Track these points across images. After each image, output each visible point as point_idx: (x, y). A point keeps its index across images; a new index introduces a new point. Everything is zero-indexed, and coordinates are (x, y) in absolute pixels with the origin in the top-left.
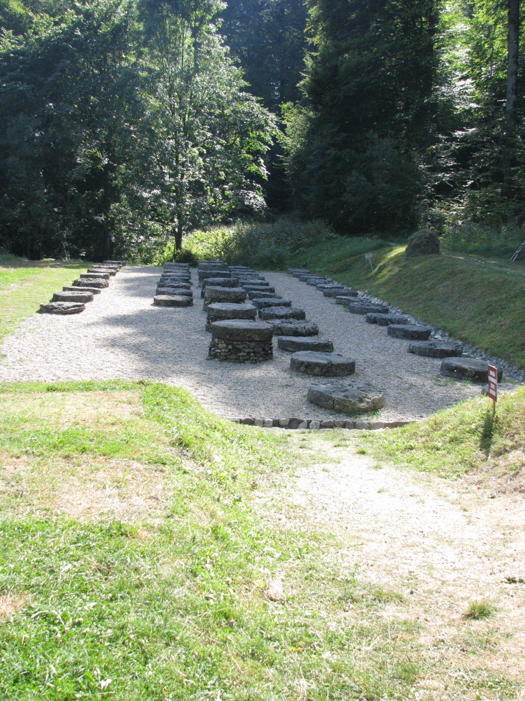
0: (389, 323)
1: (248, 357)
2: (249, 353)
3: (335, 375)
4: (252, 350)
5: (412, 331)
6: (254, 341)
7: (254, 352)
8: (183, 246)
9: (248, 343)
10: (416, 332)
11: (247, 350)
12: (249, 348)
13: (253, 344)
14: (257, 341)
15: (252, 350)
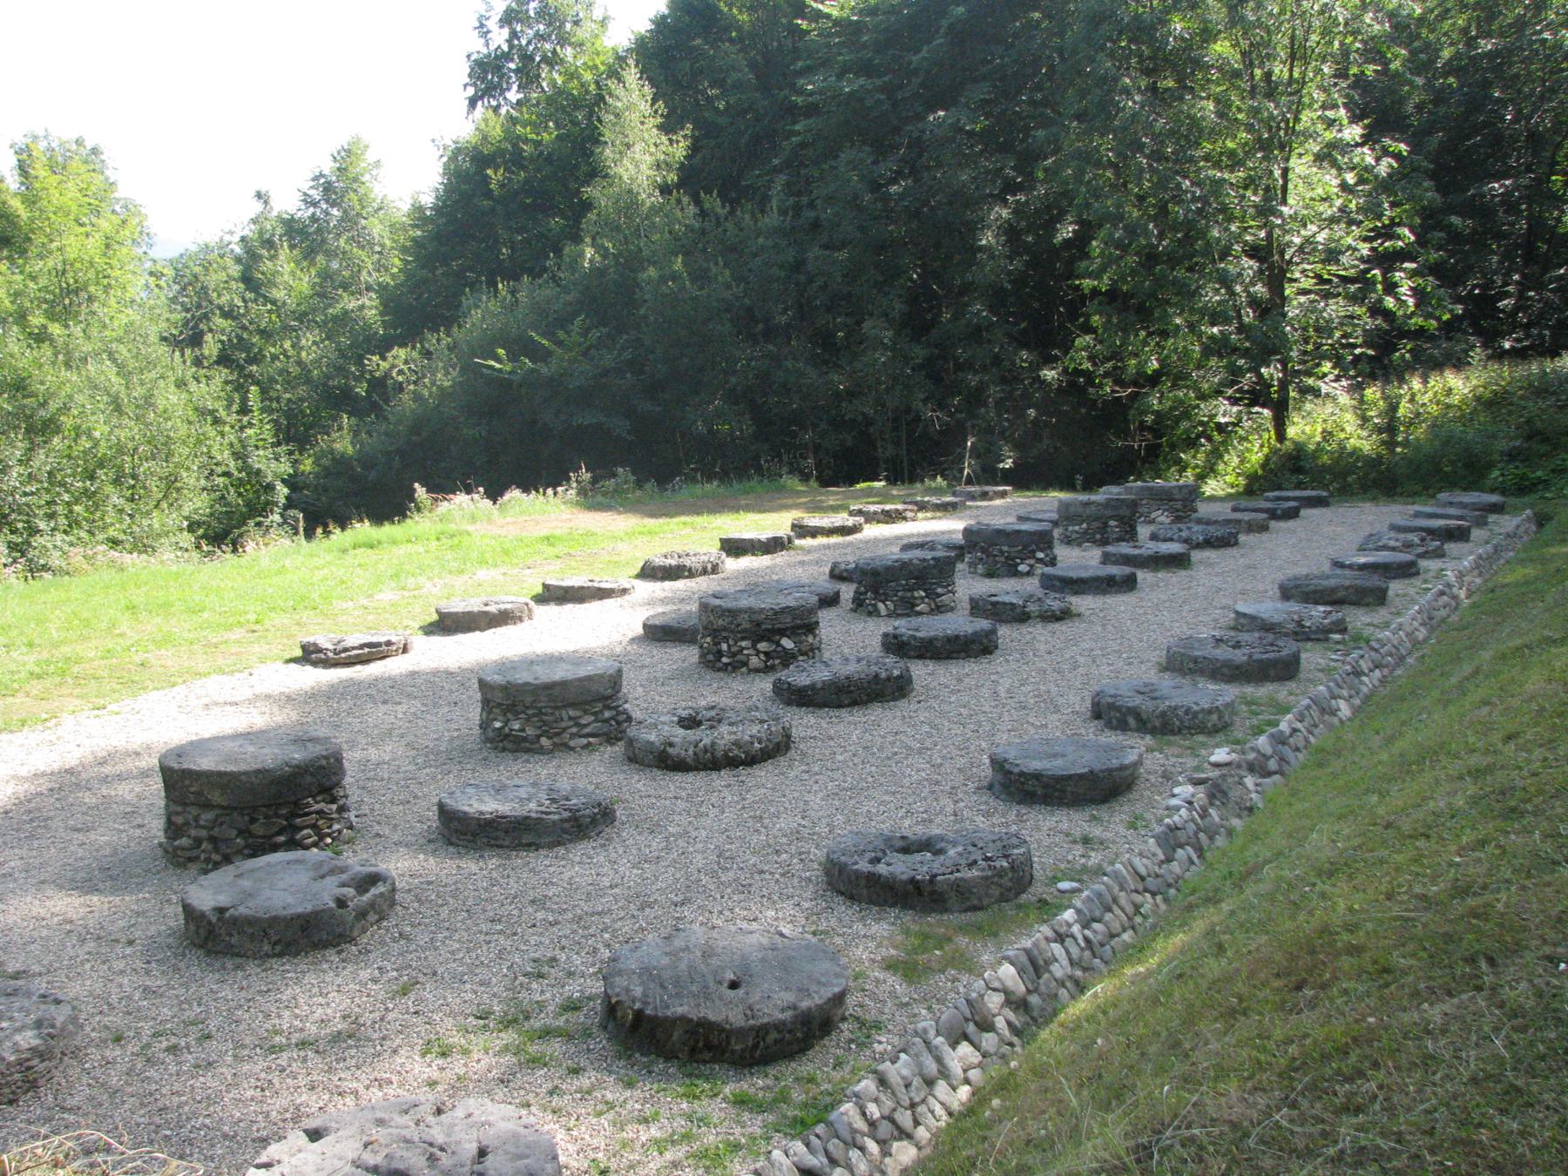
0: (1131, 721)
1: (195, 853)
2: (198, 842)
3: (230, 952)
4: (204, 833)
5: (1022, 774)
6: (207, 806)
7: (213, 839)
8: (1291, 432)
9: (194, 811)
10: (1037, 776)
11: (193, 832)
12: (198, 826)
13: (207, 816)
14: (219, 807)
15: (204, 833)
